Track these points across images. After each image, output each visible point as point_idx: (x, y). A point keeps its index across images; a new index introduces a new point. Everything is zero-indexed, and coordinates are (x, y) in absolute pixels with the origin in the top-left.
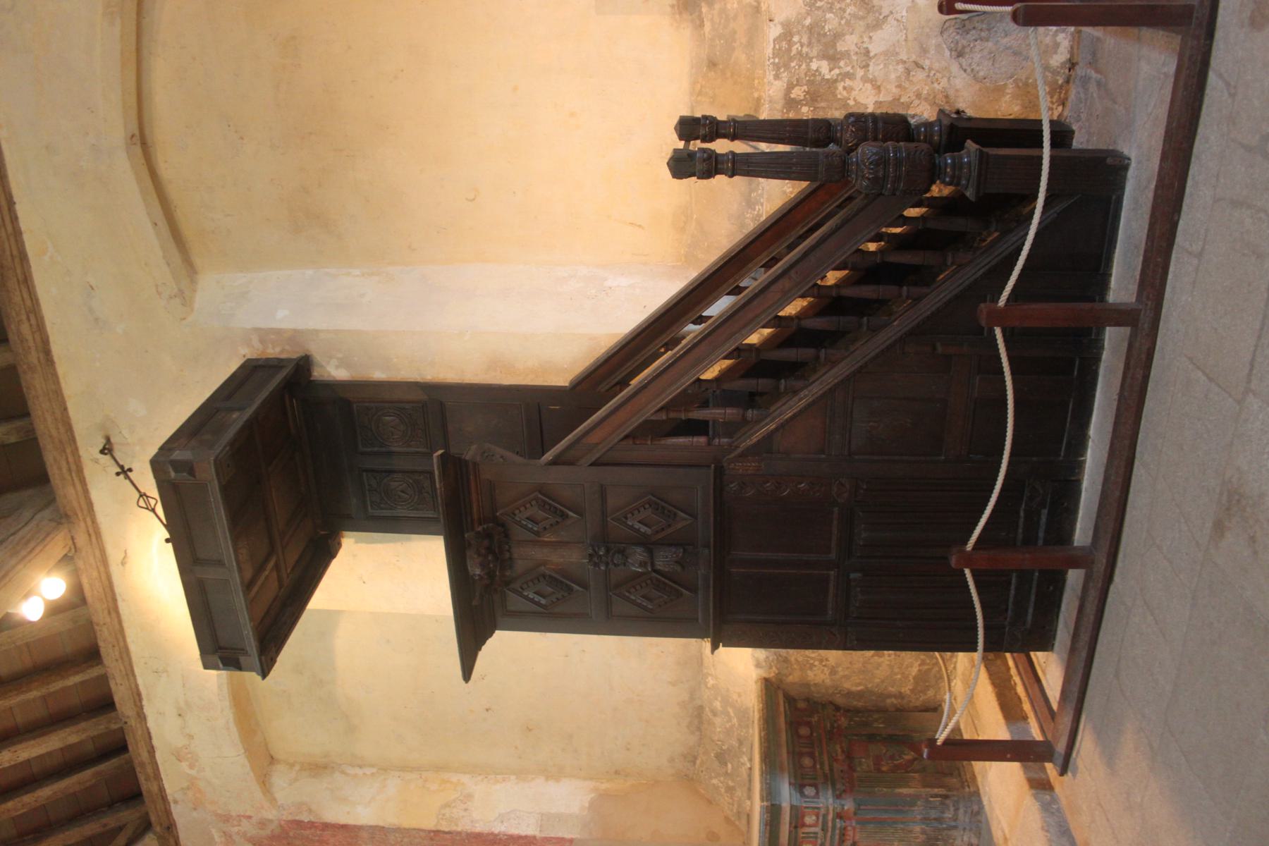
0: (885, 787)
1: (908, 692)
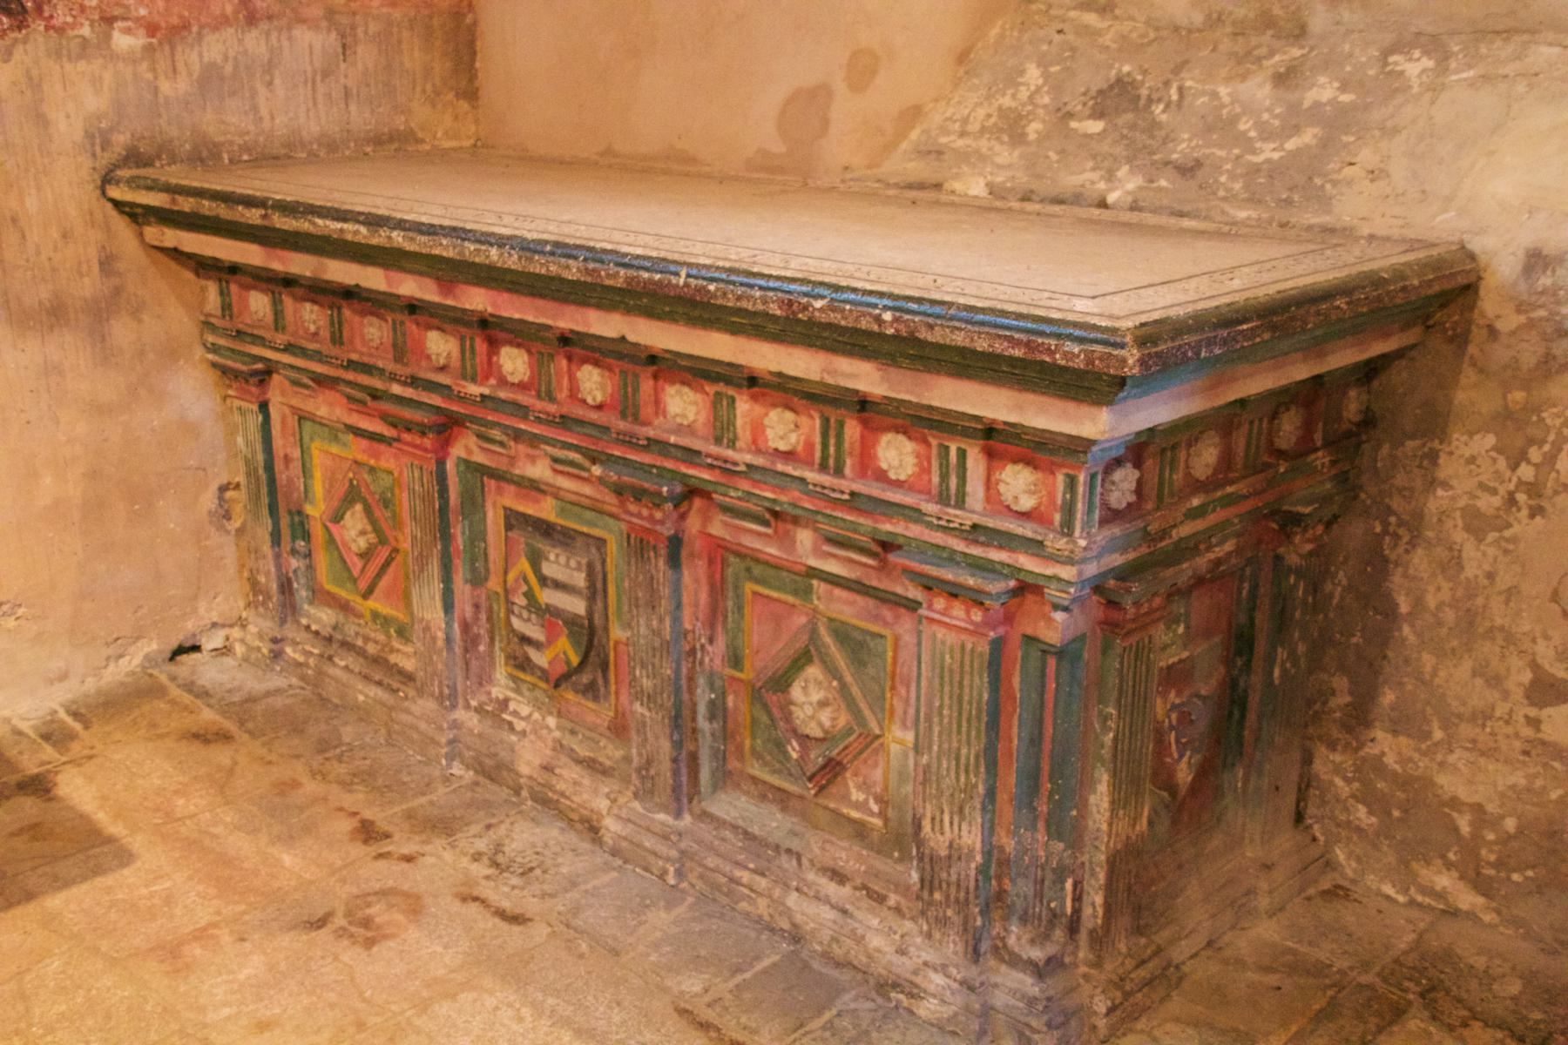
0: (1116, 739)
1: (1371, 750)
